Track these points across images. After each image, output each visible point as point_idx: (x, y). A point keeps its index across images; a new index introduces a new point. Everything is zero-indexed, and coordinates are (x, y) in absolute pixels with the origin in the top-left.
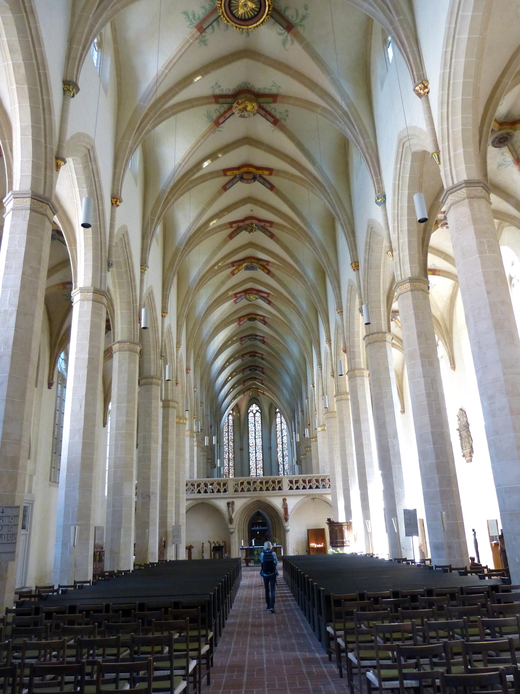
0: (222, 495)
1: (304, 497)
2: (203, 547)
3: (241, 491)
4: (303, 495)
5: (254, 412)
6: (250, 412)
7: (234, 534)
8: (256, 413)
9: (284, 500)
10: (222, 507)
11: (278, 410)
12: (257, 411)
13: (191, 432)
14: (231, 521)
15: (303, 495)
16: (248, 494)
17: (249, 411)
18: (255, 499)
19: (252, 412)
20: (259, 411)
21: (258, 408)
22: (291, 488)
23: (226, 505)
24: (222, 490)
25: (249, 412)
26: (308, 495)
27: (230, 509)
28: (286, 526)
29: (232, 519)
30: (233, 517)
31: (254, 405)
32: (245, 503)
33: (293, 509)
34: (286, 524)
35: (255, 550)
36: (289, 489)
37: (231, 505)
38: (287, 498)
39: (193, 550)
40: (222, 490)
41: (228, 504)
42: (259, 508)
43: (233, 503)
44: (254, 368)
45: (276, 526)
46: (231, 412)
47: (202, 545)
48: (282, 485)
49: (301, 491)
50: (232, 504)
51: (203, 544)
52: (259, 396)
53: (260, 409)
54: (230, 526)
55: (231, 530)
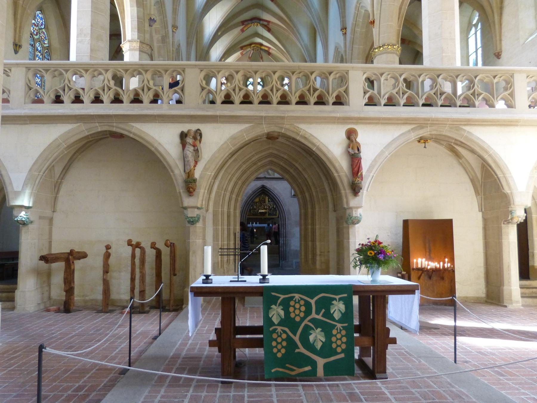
1: (409, 127)
2: (107, 256)
3: (223, 103)
4: (406, 121)
6: (249, 84)
7: (199, 225)
9: (351, 135)
10: (167, 147)
15: (406, 121)
17: (248, 83)
18: (265, 129)
20: (261, 83)
22: (371, 102)
23: (177, 140)
25: (248, 84)
26: (421, 124)
27: (190, 149)
28: (351, 208)
29: (195, 181)
30: (197, 175)
32: (233, 138)
33: (375, 161)
34: (353, 202)
35: (274, 301)
37: (189, 140)
38: (358, 128)
39: (78, 264)
41: (183, 136)
42: (271, 162)
43: (198, 135)
45: (317, 209)
46: (225, 82)
47: (104, 250)
48: (346, 91)
50: (195, 138)
51: (108, 247)
54: (188, 201)
55: (191, 213)
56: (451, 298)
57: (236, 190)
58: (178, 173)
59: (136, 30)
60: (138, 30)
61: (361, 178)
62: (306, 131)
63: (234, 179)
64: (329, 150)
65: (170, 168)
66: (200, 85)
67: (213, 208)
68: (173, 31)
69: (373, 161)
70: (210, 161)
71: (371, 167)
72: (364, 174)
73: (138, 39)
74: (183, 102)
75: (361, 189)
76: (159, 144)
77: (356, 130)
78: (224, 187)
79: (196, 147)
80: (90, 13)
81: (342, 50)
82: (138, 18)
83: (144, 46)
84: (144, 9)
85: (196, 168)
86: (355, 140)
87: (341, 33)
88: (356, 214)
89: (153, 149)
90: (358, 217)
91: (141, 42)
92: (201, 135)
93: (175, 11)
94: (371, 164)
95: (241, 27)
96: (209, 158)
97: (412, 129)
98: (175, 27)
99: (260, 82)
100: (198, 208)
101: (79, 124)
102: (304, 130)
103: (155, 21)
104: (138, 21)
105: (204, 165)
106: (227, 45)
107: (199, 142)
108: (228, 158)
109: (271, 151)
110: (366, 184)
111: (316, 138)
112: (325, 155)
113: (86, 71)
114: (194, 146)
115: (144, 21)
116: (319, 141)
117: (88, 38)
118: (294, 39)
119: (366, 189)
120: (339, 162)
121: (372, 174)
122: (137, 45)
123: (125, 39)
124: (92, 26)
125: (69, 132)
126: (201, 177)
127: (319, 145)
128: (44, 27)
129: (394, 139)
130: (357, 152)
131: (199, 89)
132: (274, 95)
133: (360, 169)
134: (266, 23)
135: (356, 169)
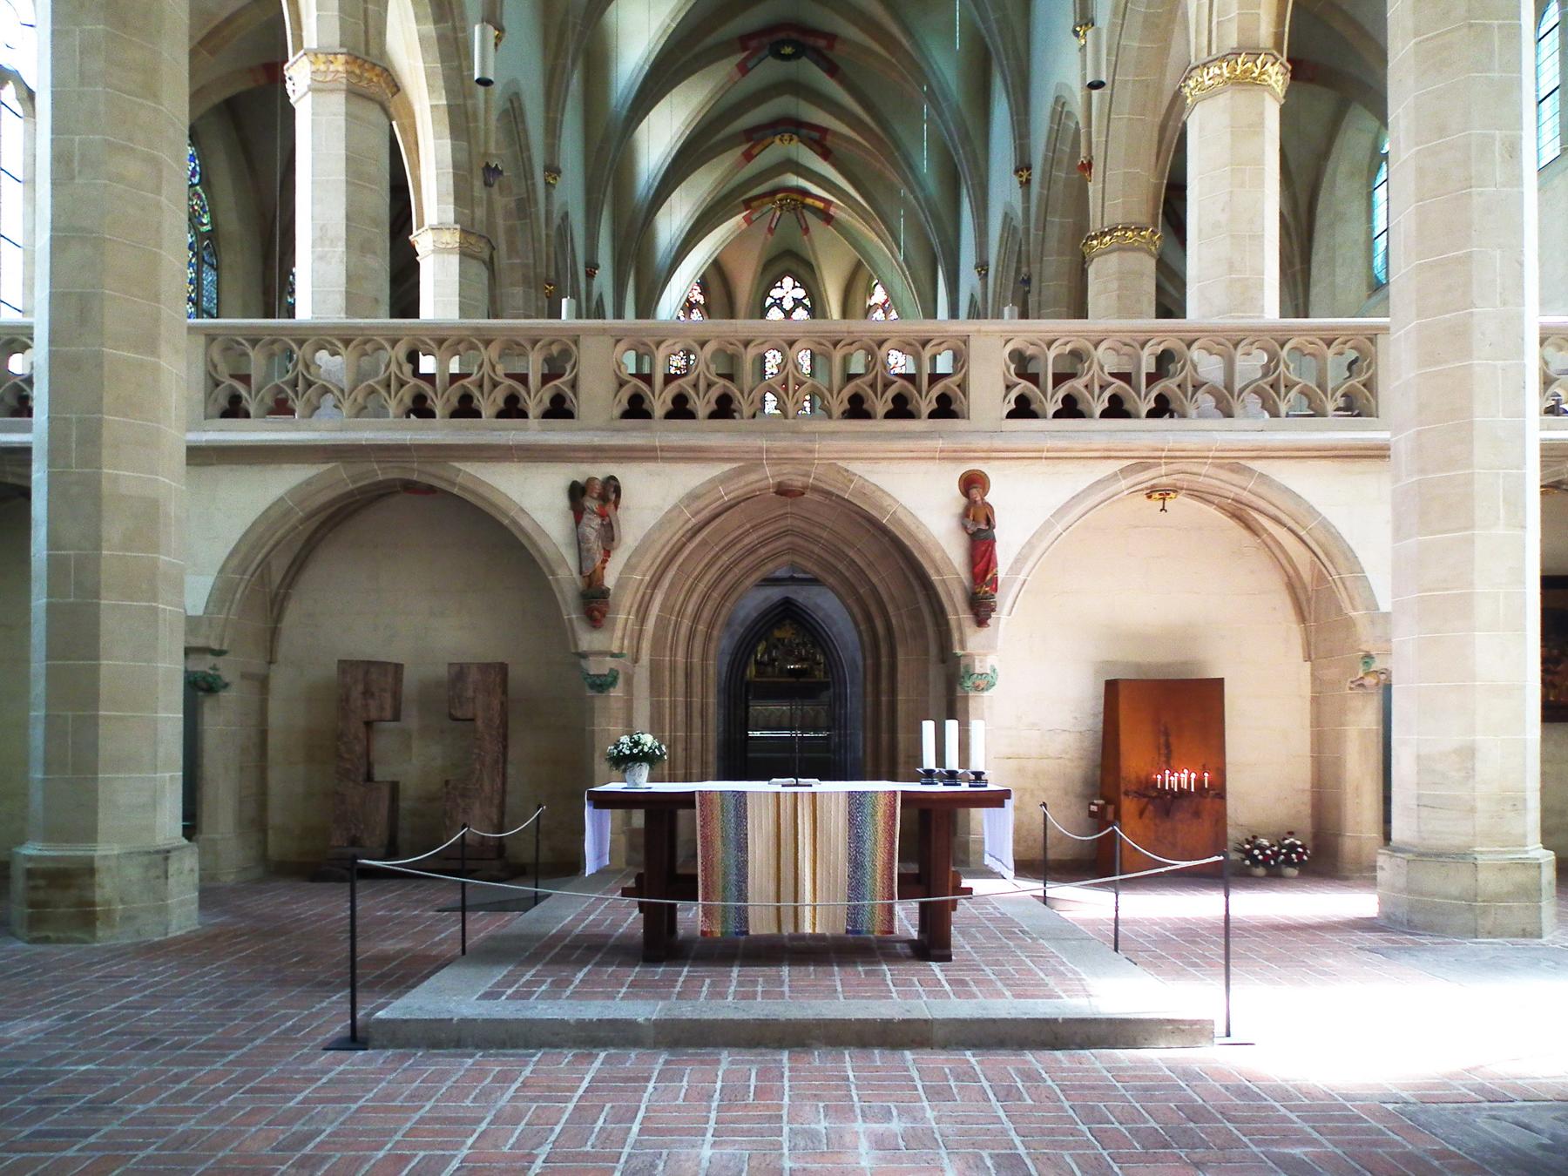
0: (533, 431)
3: (669, 415)
5: (788, 305)
6: (772, 305)
8: (793, 310)
9: (972, 484)
11: (879, 296)
12: (798, 303)
13: (354, 58)
14: (595, 602)
16: (718, 435)
17: (769, 301)
18: (769, 475)
19: (780, 306)
20: (806, 301)
21: (800, 293)
23: (563, 502)
24: (536, 401)
25: (767, 304)
29: (605, 593)
30: (610, 580)
31: (788, 281)
32: (693, 497)
36: (1011, 415)
37: (591, 503)
40: (536, 401)
41: (577, 492)
43: (611, 491)
44: (794, 36)
46: (701, 299)
49: (1096, 431)
50: (603, 498)
52: (806, 230)
53: (809, 295)
54: (589, 640)
55: (596, 667)
56: (1111, 828)
57: (706, 614)
58: (567, 573)
59: (451, 199)
62: (867, 481)
63: (701, 587)
64: (920, 524)
65: (549, 566)
66: (616, 375)
68: (547, 184)
70: (639, 551)
71: (1020, 560)
72: (1001, 576)
73: (456, 222)
74: (576, 415)
75: (993, 610)
76: (522, 510)
78: (677, 608)
80: (343, 185)
81: (1018, 221)
82: (456, 166)
83: (473, 240)
84: (469, 143)
85: (607, 565)
86: (982, 499)
87: (1016, 180)
89: (506, 522)
91: (463, 231)
92: (618, 491)
93: (552, 129)
95: (745, 147)
97: (1121, 471)
98: (553, 170)
99: (804, 298)
100: (613, 655)
101: (330, 466)
103: (501, 173)
104: (455, 175)
106: (705, 199)
107: (613, 507)
108: (684, 539)
109: (789, 521)
110: (1004, 600)
111: (889, 495)
112: (911, 535)
113: (347, 343)
114: (603, 515)
115: (471, 171)
117: (341, 248)
118: (896, 179)
119: (1006, 609)
120: (943, 551)
121: (1021, 577)
122: (452, 238)
123: (421, 224)
124: (348, 218)
125: (308, 483)
126: (621, 584)
127: (895, 512)
128: (200, 180)
130: (983, 526)
131: (614, 385)
133: (992, 565)
134: (815, 135)
135: (981, 566)
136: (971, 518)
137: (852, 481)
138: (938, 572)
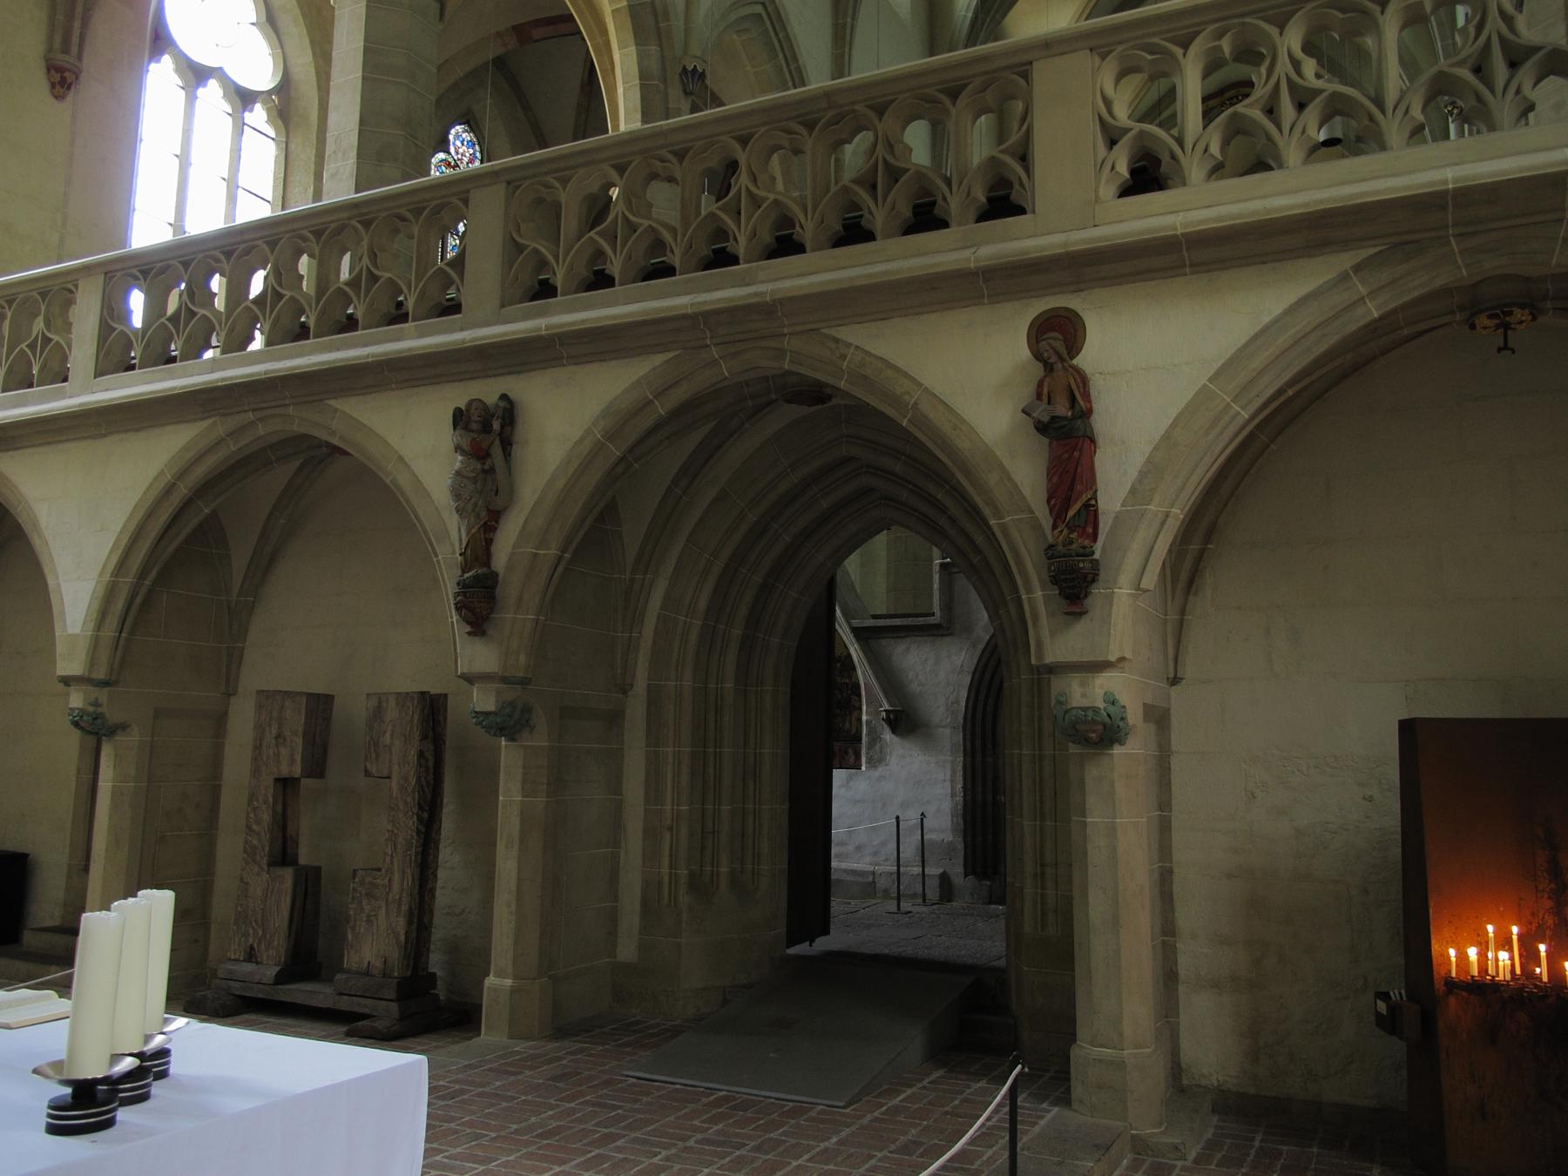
36: (1126, 191)
60: (643, 113)
61: (1090, 530)
62: (867, 352)
64: (958, 420)
67: (650, 679)
69: (1156, 448)
76: (401, 459)
77: (1078, 315)
79: (489, 462)
88: (1084, 695)
90: (1096, 710)
94: (1149, 461)
96: (536, 496)
97: (1357, 268)
101: (210, 421)
102: (857, 347)
105: (521, 521)
111: (906, 375)
116: (920, 385)
120: (1001, 466)
127: (916, 404)
129: (1265, 330)
132: (742, 230)
136: (1045, 398)
137: (843, 357)
138: (998, 514)
